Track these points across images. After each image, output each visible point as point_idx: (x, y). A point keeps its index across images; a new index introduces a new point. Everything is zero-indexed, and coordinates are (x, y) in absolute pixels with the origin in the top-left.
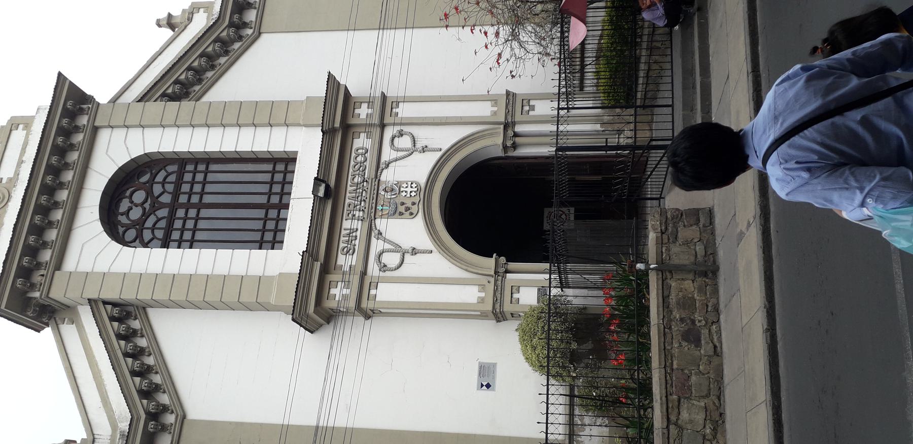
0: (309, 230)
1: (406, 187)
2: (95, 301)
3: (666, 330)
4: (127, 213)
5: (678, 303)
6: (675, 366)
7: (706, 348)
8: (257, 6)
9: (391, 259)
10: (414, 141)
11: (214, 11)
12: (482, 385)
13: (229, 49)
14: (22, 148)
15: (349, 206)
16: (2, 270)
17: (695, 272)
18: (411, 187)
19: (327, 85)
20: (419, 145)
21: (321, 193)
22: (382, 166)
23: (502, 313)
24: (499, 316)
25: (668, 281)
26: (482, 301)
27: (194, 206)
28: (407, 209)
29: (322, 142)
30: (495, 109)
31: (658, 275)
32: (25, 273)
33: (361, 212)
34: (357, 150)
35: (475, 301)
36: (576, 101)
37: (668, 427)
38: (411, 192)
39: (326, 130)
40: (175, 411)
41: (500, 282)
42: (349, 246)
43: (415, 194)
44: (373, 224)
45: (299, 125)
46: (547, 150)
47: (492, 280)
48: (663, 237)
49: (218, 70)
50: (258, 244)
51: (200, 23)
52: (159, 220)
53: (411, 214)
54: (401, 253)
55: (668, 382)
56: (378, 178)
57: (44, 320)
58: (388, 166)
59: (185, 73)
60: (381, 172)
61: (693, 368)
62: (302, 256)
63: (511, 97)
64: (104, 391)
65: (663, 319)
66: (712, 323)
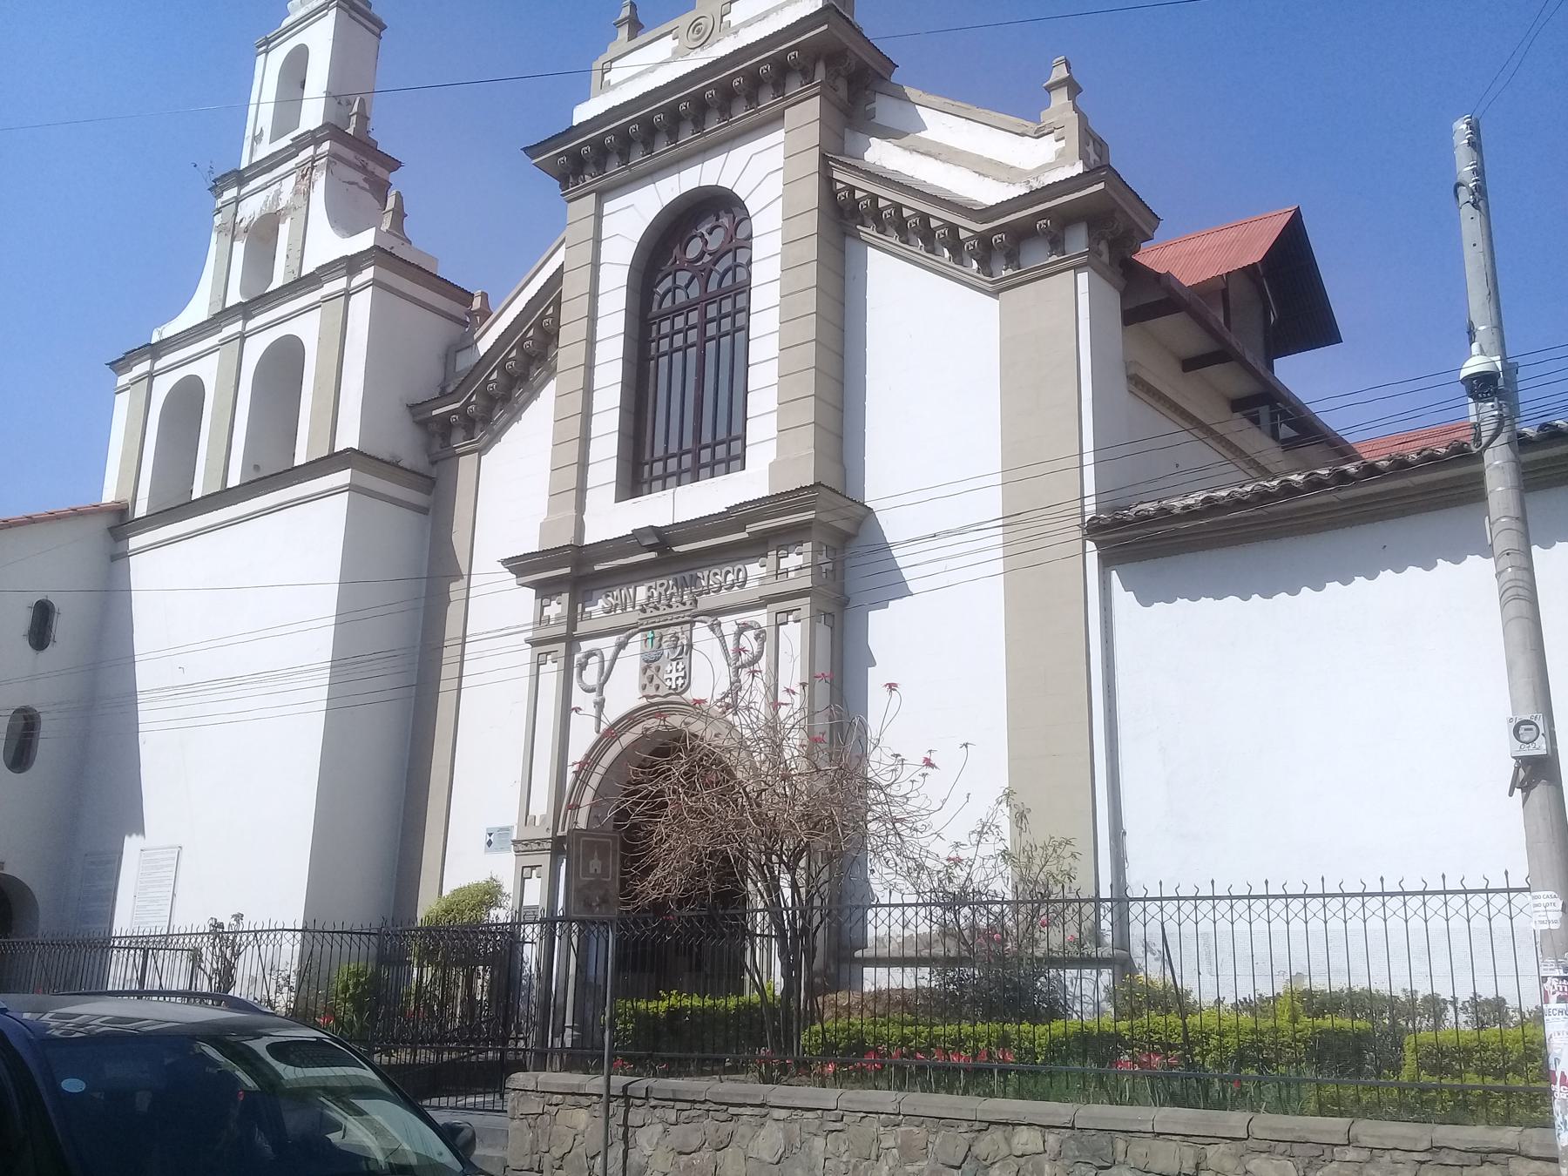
1: (677, 670)
11: (1046, 174)
12: (490, 835)
18: (677, 678)
28: (651, 680)
38: (671, 679)
44: (634, 630)
53: (644, 687)
56: (695, 619)
58: (713, 630)
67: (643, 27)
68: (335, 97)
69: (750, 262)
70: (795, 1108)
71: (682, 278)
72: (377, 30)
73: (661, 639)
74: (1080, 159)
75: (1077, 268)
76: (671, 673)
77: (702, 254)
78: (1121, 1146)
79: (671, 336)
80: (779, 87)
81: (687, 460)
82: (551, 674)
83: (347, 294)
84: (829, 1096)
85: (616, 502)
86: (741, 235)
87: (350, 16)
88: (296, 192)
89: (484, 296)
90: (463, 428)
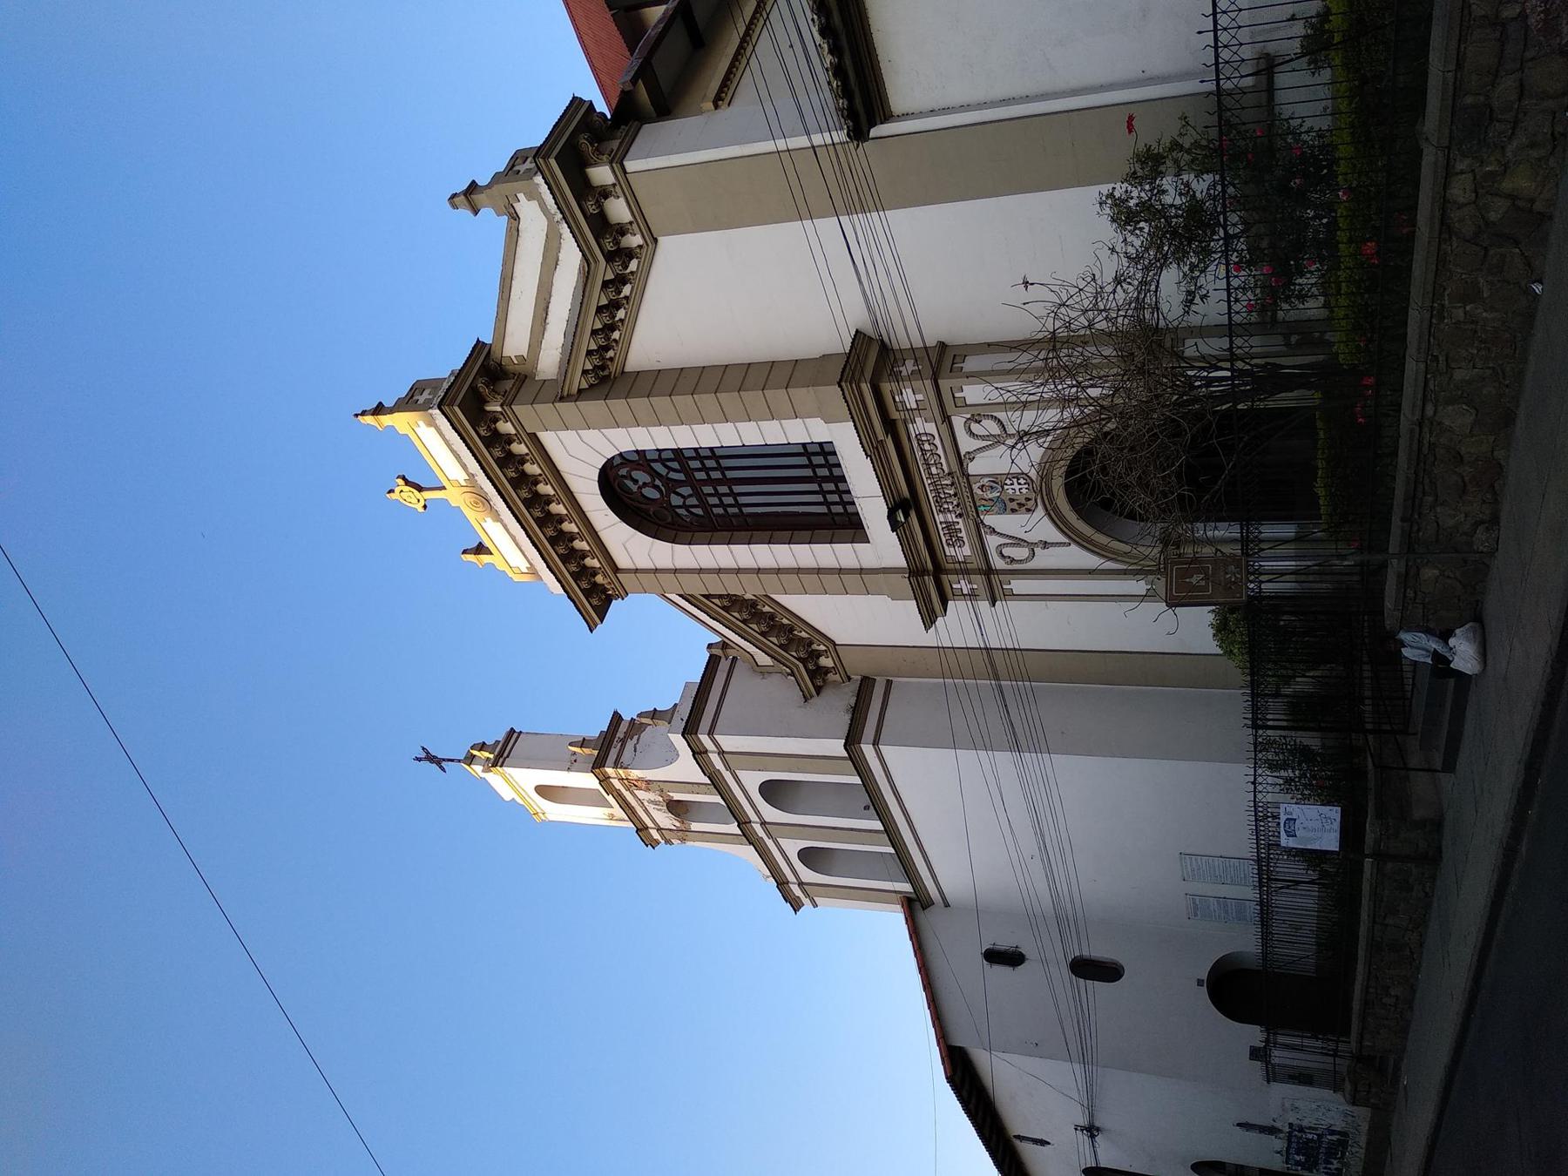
1: (1012, 484)
10: (1003, 426)
18: (1019, 484)
28: (1021, 505)
38: (1020, 489)
53: (1028, 510)
58: (974, 458)
67: (480, 543)
68: (572, 765)
69: (657, 450)
70: (1424, 396)
71: (676, 500)
72: (515, 735)
73: (985, 500)
74: (531, 179)
75: (625, 172)
76: (1016, 489)
77: (656, 487)
78: (1469, 100)
79: (722, 505)
80: (509, 440)
81: (830, 486)
82: (1018, 585)
83: (721, 753)
84: (1412, 368)
85: (869, 542)
86: (636, 457)
87: (508, 756)
88: (648, 790)
89: (710, 646)
90: (818, 658)
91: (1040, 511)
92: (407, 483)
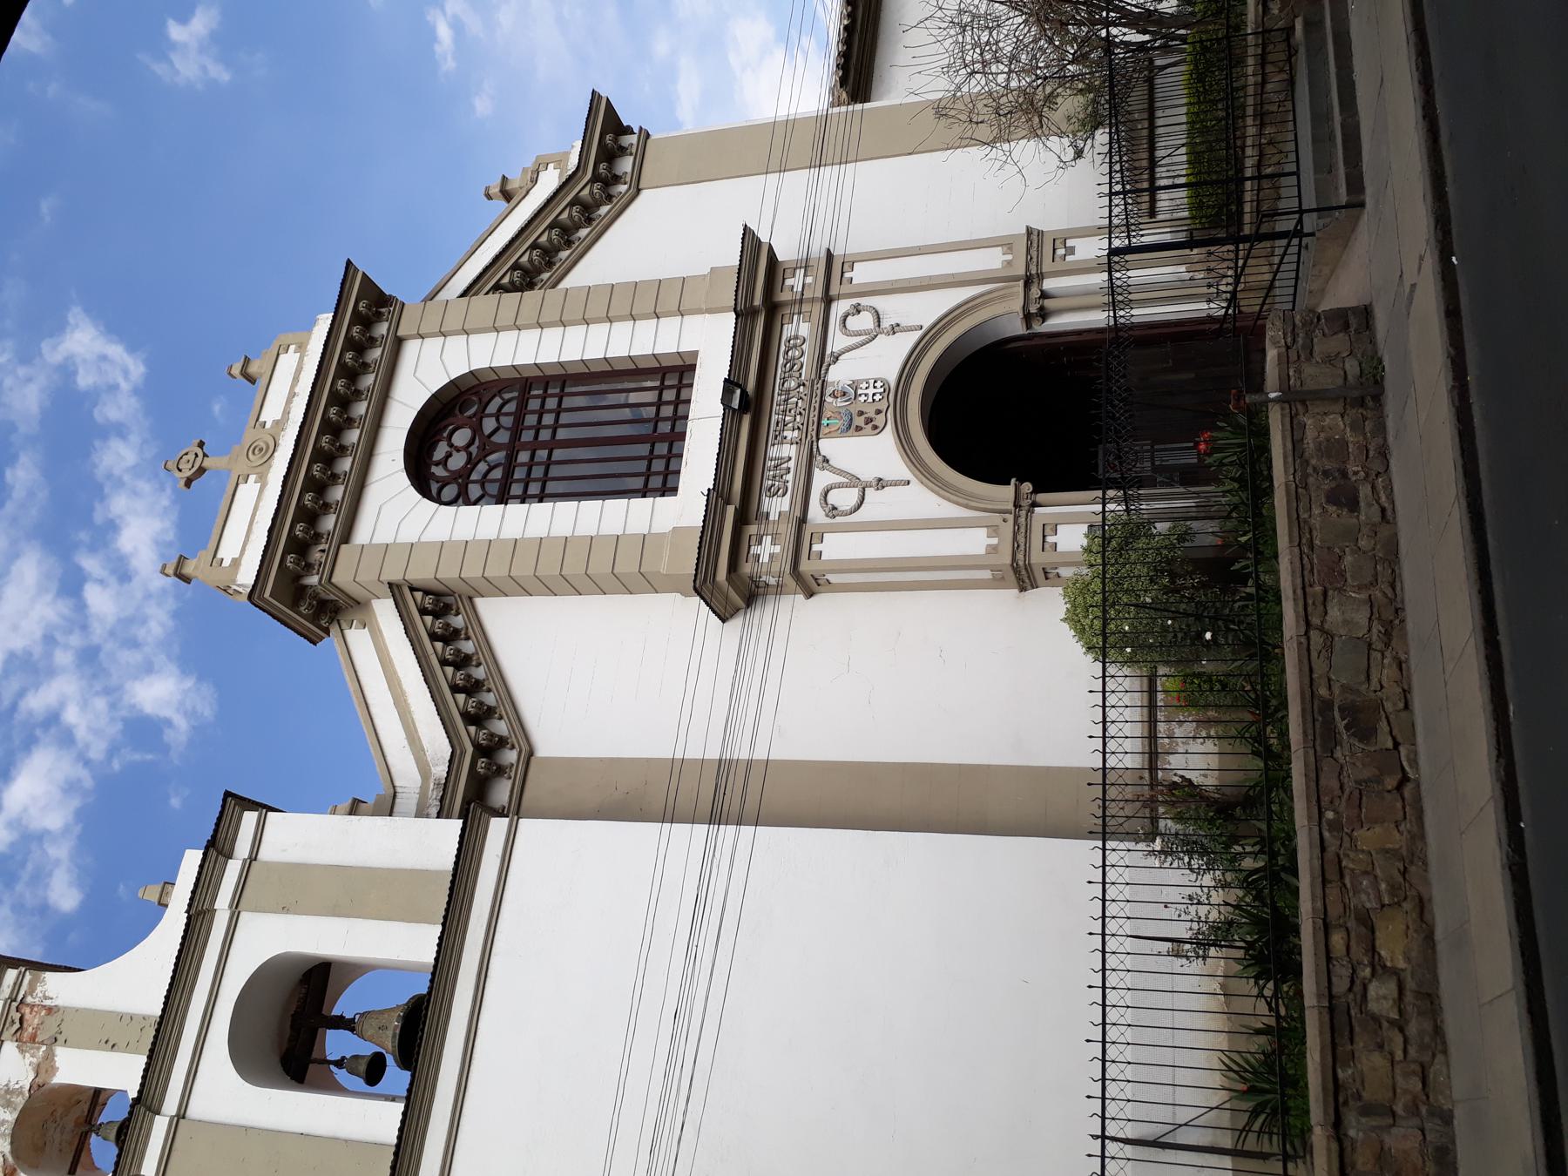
0: (717, 459)
1: (866, 388)
2: (399, 586)
3: (1300, 490)
4: (444, 462)
5: (1319, 449)
6: (1317, 542)
7: (1368, 513)
8: (634, 151)
9: (844, 498)
10: (879, 318)
13: (593, 216)
14: (294, 378)
15: (777, 425)
16: (267, 542)
17: (1345, 399)
18: (875, 387)
19: (742, 243)
20: (886, 324)
21: (736, 404)
22: (827, 359)
23: (1028, 567)
24: (1024, 576)
25: (1301, 417)
26: (992, 550)
27: (544, 445)
28: (869, 421)
29: (736, 328)
30: (1009, 257)
31: (1282, 409)
32: (299, 547)
33: (796, 431)
34: (789, 342)
35: (982, 551)
36: (1142, 236)
37: (1307, 633)
38: (874, 395)
39: (741, 310)
40: (517, 746)
41: (1024, 519)
42: (777, 483)
43: (881, 397)
44: (815, 447)
45: (699, 311)
46: (1098, 318)
47: (1010, 517)
48: (1290, 354)
49: (577, 247)
50: (640, 495)
51: (549, 182)
52: (491, 469)
53: (875, 427)
54: (860, 488)
55: (1305, 567)
57: (322, 622)
58: (837, 359)
59: (528, 252)
60: (827, 370)
61: (1347, 544)
62: (708, 495)
63: (1034, 237)
64: (410, 721)
65: (1294, 474)
66: (1377, 476)
83: (253, 857)
88: (26, 1040)
91: (888, 436)
92: (201, 444)
